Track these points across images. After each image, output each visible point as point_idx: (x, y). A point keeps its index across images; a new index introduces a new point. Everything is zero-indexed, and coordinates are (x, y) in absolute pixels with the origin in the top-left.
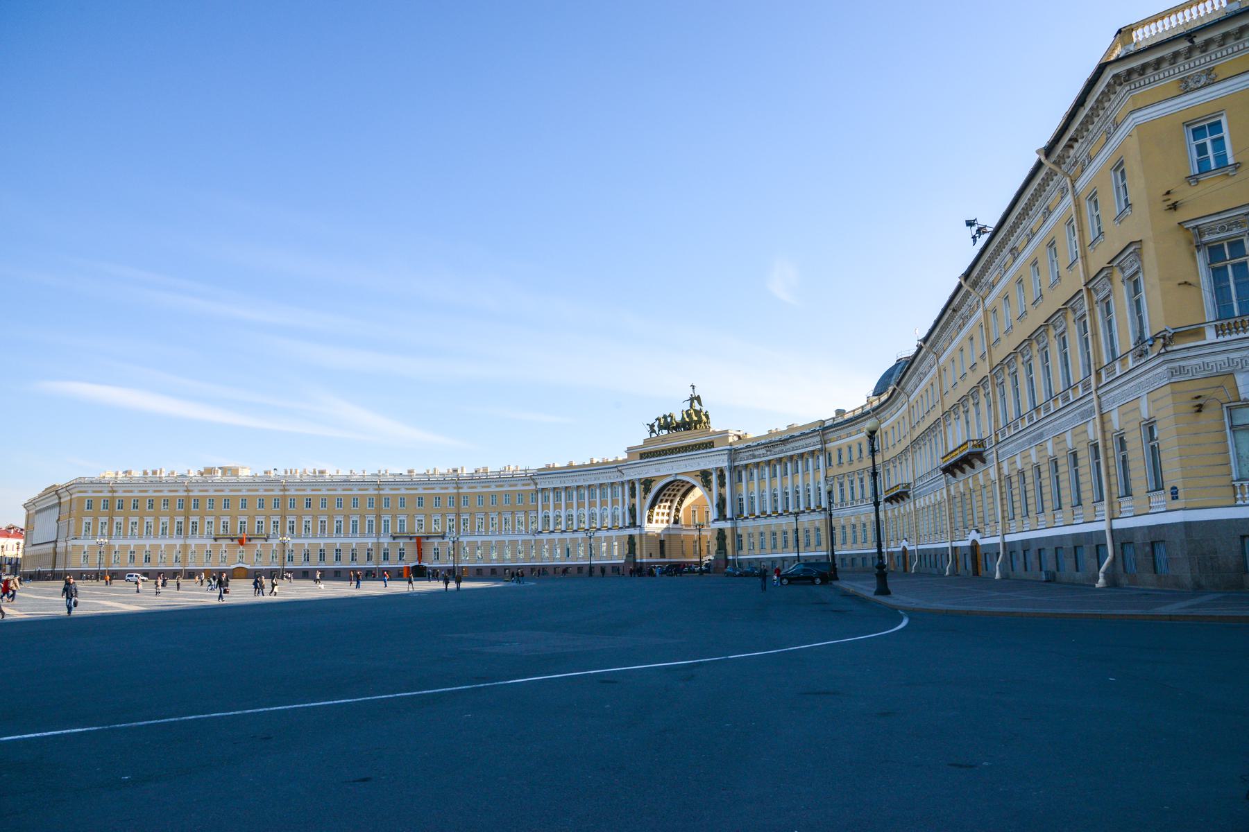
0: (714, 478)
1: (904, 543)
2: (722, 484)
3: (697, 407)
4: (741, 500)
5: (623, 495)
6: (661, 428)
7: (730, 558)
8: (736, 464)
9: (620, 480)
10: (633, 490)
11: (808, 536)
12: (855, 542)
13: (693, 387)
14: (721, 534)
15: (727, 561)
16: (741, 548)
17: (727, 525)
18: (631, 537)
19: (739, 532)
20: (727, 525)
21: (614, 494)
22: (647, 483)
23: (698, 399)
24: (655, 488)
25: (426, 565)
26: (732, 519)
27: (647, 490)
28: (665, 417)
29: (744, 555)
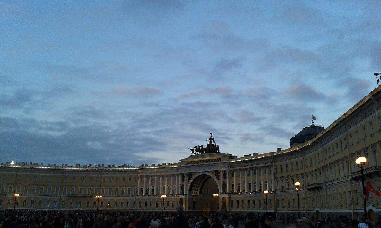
0: (221, 174)
1: (317, 209)
2: (225, 177)
3: (213, 143)
4: (233, 185)
5: (178, 180)
6: (196, 151)
7: (228, 211)
8: (231, 169)
11: (289, 203)
12: (289, 207)
15: (226, 212)
16: (232, 206)
17: (226, 196)
18: (181, 199)
19: (232, 199)
20: (226, 196)
21: (174, 180)
22: (190, 175)
25: (83, 210)
26: (229, 193)
27: (189, 178)
29: (234, 210)
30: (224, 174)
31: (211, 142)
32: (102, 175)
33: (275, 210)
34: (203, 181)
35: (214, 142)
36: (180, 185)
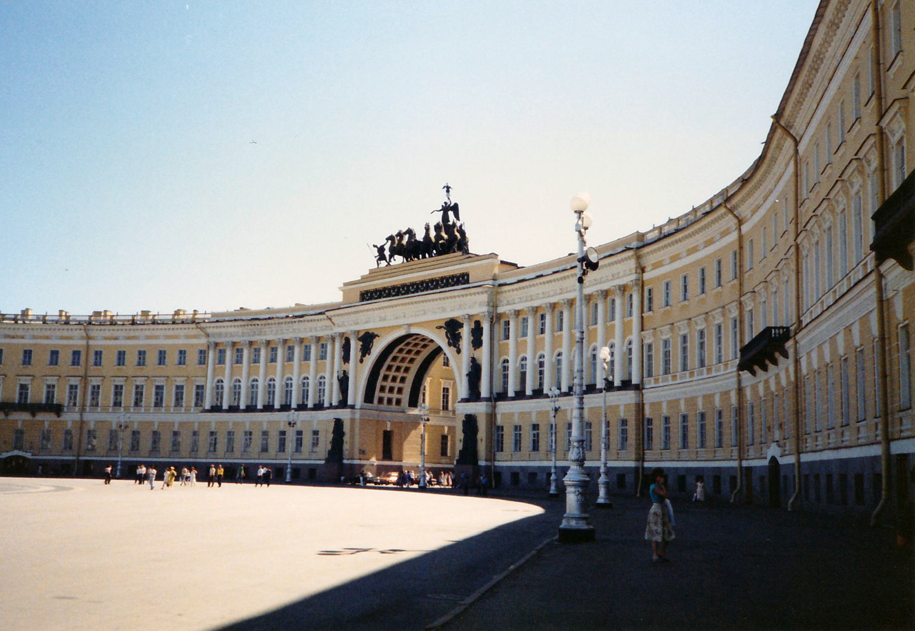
0: (465, 332)
2: (477, 343)
6: (394, 251)
9: (329, 333)
10: (346, 348)
13: (448, 189)
14: (470, 422)
17: (479, 409)
20: (479, 409)
22: (367, 339)
23: (455, 208)
24: (378, 347)
25: (28, 455)
26: (488, 400)
27: (366, 350)
28: (400, 235)
29: (507, 460)
30: (477, 332)
31: (445, 218)
32: (91, 342)
33: (637, 460)
34: (420, 359)
35: (457, 216)
36: (335, 375)
